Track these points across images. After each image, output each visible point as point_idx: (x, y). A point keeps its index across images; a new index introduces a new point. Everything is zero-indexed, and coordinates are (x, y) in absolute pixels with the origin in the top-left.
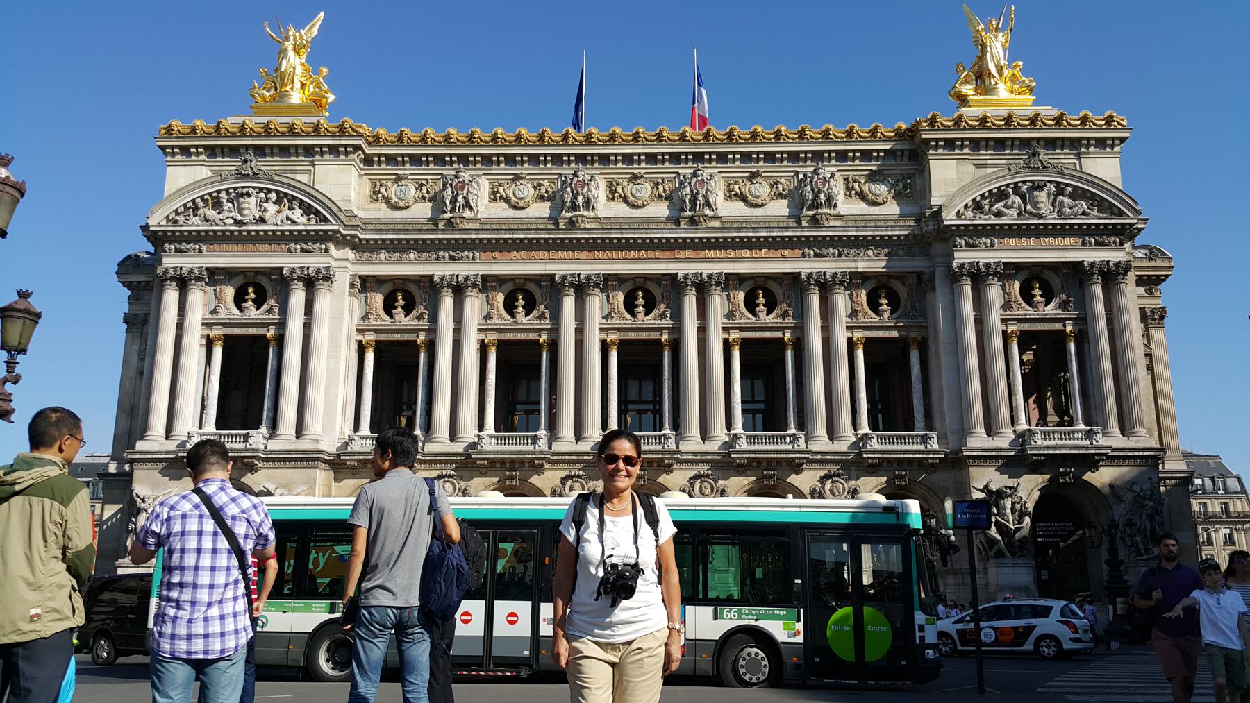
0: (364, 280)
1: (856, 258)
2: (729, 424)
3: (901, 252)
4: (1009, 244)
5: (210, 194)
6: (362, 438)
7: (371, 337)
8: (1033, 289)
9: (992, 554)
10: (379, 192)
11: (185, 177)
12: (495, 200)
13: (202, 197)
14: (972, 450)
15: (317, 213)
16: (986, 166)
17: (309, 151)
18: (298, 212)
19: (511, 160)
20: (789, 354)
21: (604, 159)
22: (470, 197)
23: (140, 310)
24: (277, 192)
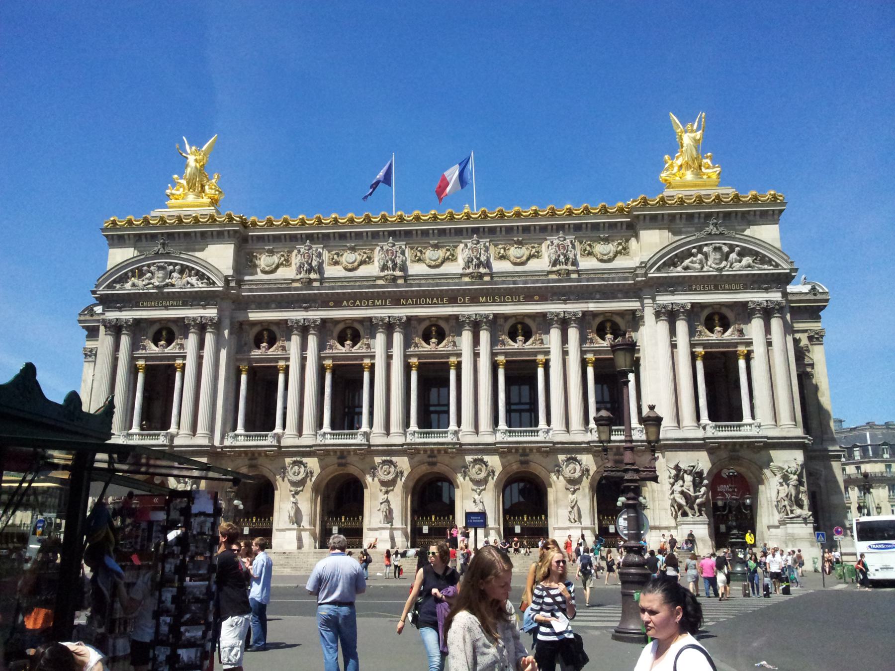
0: (241, 324)
2: (496, 422)
3: (619, 295)
5: (137, 268)
6: (237, 436)
9: (679, 514)
11: (120, 255)
13: (132, 271)
14: (667, 440)
17: (203, 234)
19: (343, 236)
20: (540, 371)
22: (314, 263)
24: (182, 265)
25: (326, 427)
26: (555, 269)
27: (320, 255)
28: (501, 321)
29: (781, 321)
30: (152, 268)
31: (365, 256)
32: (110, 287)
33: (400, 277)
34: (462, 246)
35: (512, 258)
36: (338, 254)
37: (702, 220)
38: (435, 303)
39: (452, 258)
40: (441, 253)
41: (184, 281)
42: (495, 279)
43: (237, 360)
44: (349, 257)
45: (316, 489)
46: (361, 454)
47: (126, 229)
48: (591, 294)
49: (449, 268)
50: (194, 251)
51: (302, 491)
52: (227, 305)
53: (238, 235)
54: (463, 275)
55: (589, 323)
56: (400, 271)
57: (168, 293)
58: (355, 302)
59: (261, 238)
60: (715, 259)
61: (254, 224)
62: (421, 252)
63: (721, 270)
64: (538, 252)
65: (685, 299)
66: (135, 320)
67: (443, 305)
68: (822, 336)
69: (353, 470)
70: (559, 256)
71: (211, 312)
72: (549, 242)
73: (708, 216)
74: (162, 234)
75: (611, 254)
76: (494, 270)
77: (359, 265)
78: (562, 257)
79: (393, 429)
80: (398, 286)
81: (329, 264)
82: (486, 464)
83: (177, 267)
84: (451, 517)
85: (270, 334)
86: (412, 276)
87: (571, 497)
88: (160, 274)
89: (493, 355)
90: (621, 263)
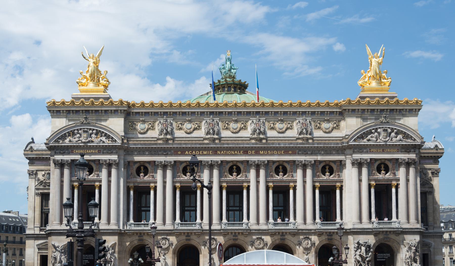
0: (129, 162)
1: (316, 154)
3: (334, 152)
4: (373, 151)
5: (71, 131)
7: (131, 185)
8: (381, 167)
10: (132, 127)
13: (68, 132)
15: (112, 138)
17: (106, 111)
20: (291, 192)
21: (221, 113)
22: (169, 130)
23: (34, 168)
24: (97, 130)
25: (178, 220)
26: (300, 136)
27: (171, 124)
28: (271, 164)
29: (414, 169)
30: (80, 131)
31: (197, 126)
32: (56, 141)
33: (217, 139)
34: (250, 122)
35: (278, 129)
36: (181, 124)
37: (379, 113)
38: (236, 154)
39: (245, 128)
40: (239, 125)
41: (99, 139)
42: (269, 142)
44: (187, 126)
45: (174, 253)
46: (198, 235)
47: (61, 107)
48: (319, 151)
49: (243, 134)
50: (101, 120)
51: (167, 253)
52: (122, 152)
53: (125, 112)
54: (251, 139)
55: (317, 166)
56: (217, 135)
57: (90, 146)
58: (192, 152)
60: (384, 136)
61: (134, 105)
62: (228, 124)
63: (386, 142)
64: (291, 126)
65: (367, 156)
66: (71, 160)
67: (241, 155)
68: (438, 172)
69: (193, 243)
70: (303, 130)
71: (114, 157)
72: (297, 121)
73: (382, 110)
74: (82, 110)
75: (330, 129)
76: (268, 135)
77: (194, 130)
78: (304, 130)
80: (216, 144)
81: (177, 130)
83: (94, 131)
85: (143, 168)
86: (223, 137)
88: (85, 135)
89: (267, 182)
90: (335, 134)
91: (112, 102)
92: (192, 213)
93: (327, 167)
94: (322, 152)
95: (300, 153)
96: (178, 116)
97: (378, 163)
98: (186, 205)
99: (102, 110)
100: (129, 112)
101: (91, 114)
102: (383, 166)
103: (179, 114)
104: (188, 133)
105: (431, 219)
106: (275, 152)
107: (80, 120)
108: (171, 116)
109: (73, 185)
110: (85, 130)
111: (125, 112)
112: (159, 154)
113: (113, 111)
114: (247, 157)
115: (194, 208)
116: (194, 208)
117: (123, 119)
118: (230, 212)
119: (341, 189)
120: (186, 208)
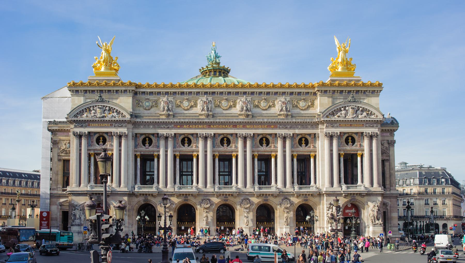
0: (136, 134)
1: (294, 128)
3: (309, 127)
5: (88, 108)
7: (138, 153)
8: (349, 139)
10: (139, 104)
12: (177, 107)
13: (85, 109)
16: (337, 99)
17: (117, 91)
18: (115, 114)
19: (182, 93)
20: (273, 160)
24: (109, 107)
32: (75, 116)
37: (347, 94)
43: (135, 151)
46: (195, 196)
50: (113, 99)
52: (130, 126)
53: (133, 92)
54: (240, 115)
59: (143, 93)
68: (394, 143)
71: (124, 130)
74: (97, 90)
78: (284, 108)
79: (208, 185)
80: (209, 119)
82: (249, 200)
83: (107, 108)
84: (233, 223)
85: (147, 140)
87: (286, 215)
91: (123, 84)
92: (189, 177)
93: (303, 139)
94: (300, 127)
95: (281, 127)
96: (177, 95)
97: (346, 136)
98: (184, 171)
99: (113, 90)
100: (137, 91)
101: (104, 93)
102: (350, 139)
103: (178, 94)
104: (186, 110)
105: (388, 182)
106: (260, 126)
107: (94, 98)
108: (172, 95)
109: (89, 153)
110: (99, 107)
111: (133, 92)
112: (161, 128)
113: (123, 91)
114: (236, 131)
115: (190, 173)
116: (190, 173)
117: (131, 98)
118: (221, 177)
119: (315, 157)
120: (184, 173)
